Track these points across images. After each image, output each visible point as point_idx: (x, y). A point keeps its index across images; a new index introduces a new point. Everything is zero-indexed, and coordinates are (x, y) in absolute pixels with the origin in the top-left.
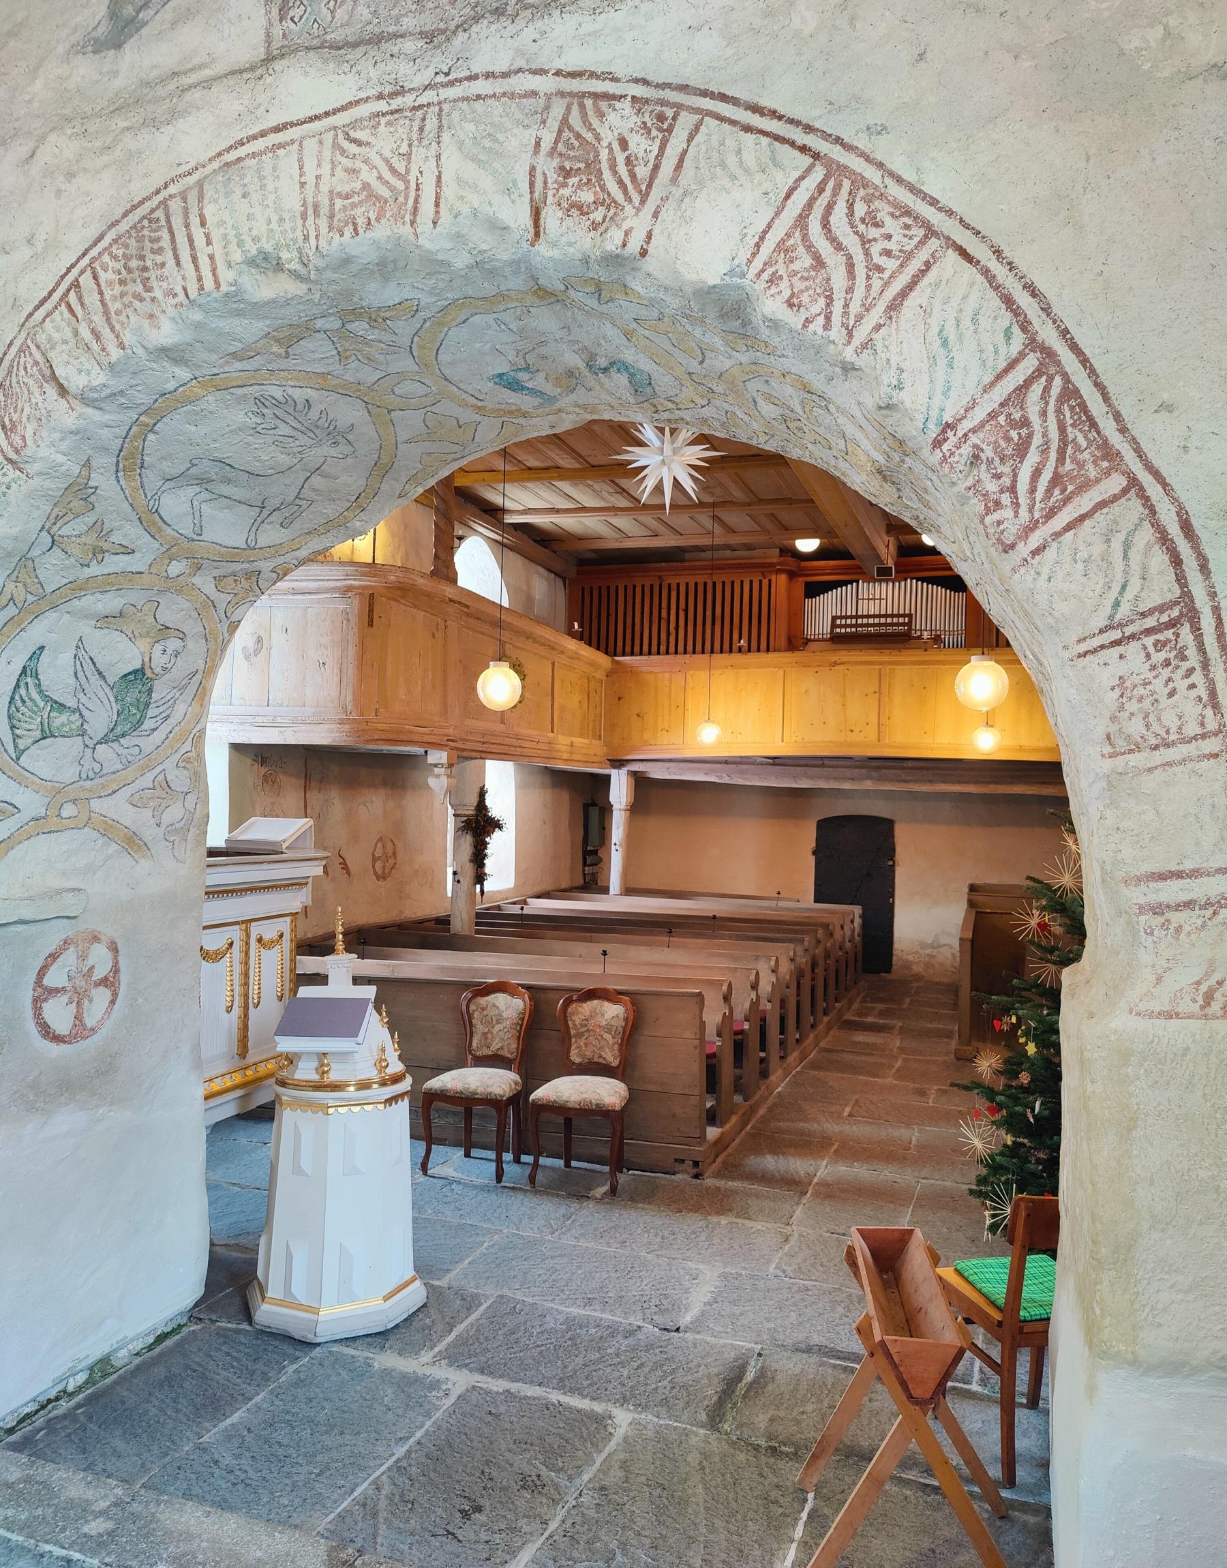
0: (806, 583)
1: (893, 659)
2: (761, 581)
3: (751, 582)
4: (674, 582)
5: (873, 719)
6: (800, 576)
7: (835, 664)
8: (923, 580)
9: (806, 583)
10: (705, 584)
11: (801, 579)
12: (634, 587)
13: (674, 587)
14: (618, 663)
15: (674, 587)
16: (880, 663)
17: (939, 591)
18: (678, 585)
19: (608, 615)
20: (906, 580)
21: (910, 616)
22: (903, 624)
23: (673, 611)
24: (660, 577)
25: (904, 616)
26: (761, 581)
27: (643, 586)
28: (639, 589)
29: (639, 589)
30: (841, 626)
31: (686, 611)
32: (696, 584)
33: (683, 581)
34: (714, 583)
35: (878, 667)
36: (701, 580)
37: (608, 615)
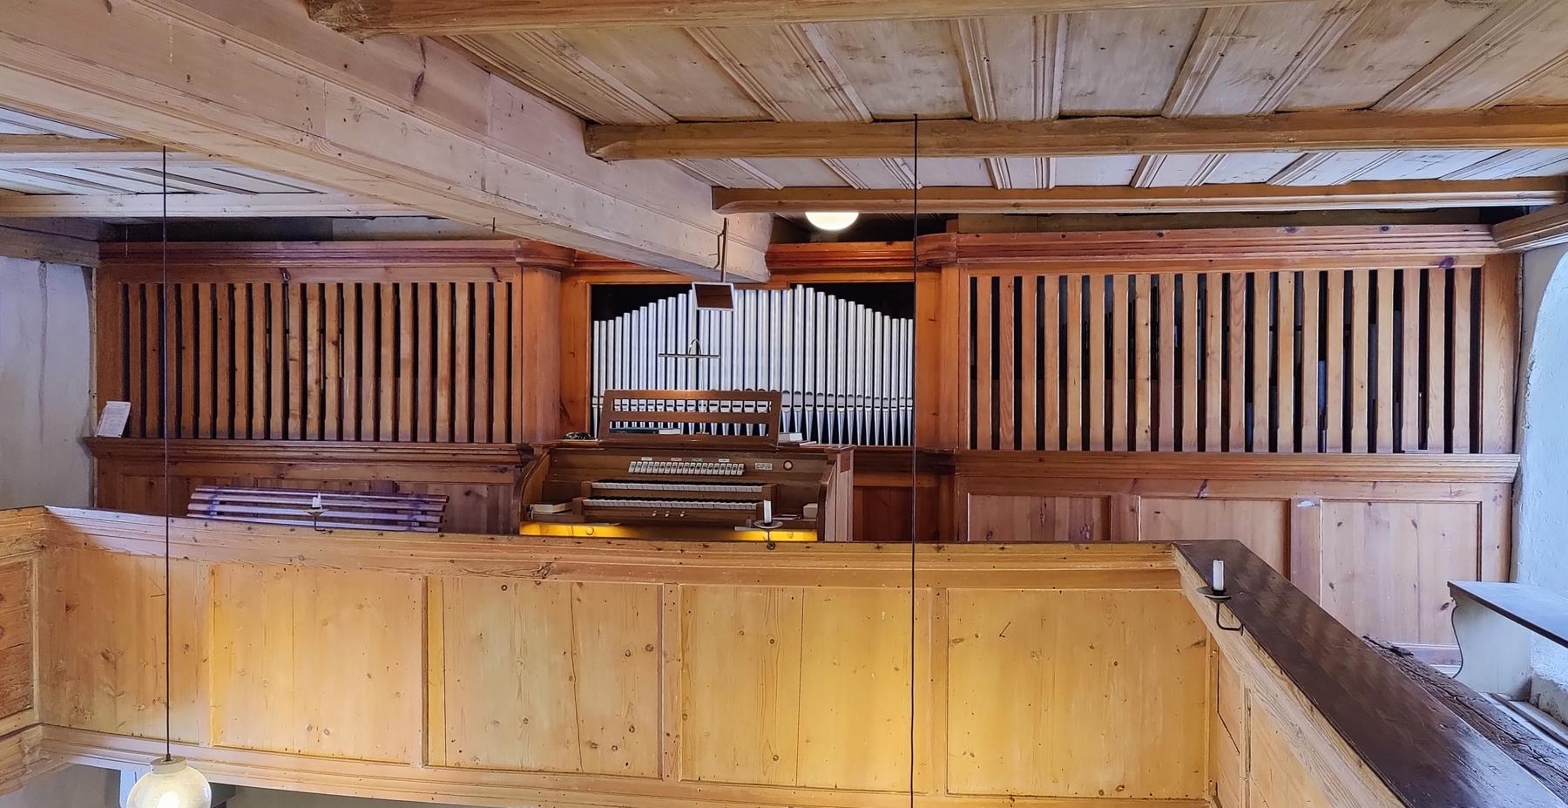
0: (595, 288)
1: (695, 563)
2: (490, 285)
3: (472, 286)
4: (312, 281)
5: (645, 716)
6: (578, 273)
7: (545, 571)
8: (828, 289)
9: (595, 288)
10: (377, 287)
11: (582, 280)
12: (232, 289)
13: (313, 292)
14: (57, 520)
15: (313, 292)
16: (659, 574)
17: (860, 315)
18: (322, 286)
19: (180, 348)
20: (793, 287)
21: (774, 397)
22: (756, 418)
23: (312, 345)
24: (283, 270)
25: (757, 395)
26: (490, 285)
27: (249, 287)
28: (240, 295)
29: (240, 295)
30: (622, 416)
31: (339, 344)
32: (359, 287)
33: (331, 280)
34: (396, 287)
35: (654, 583)
36: (368, 278)
37: (180, 348)
